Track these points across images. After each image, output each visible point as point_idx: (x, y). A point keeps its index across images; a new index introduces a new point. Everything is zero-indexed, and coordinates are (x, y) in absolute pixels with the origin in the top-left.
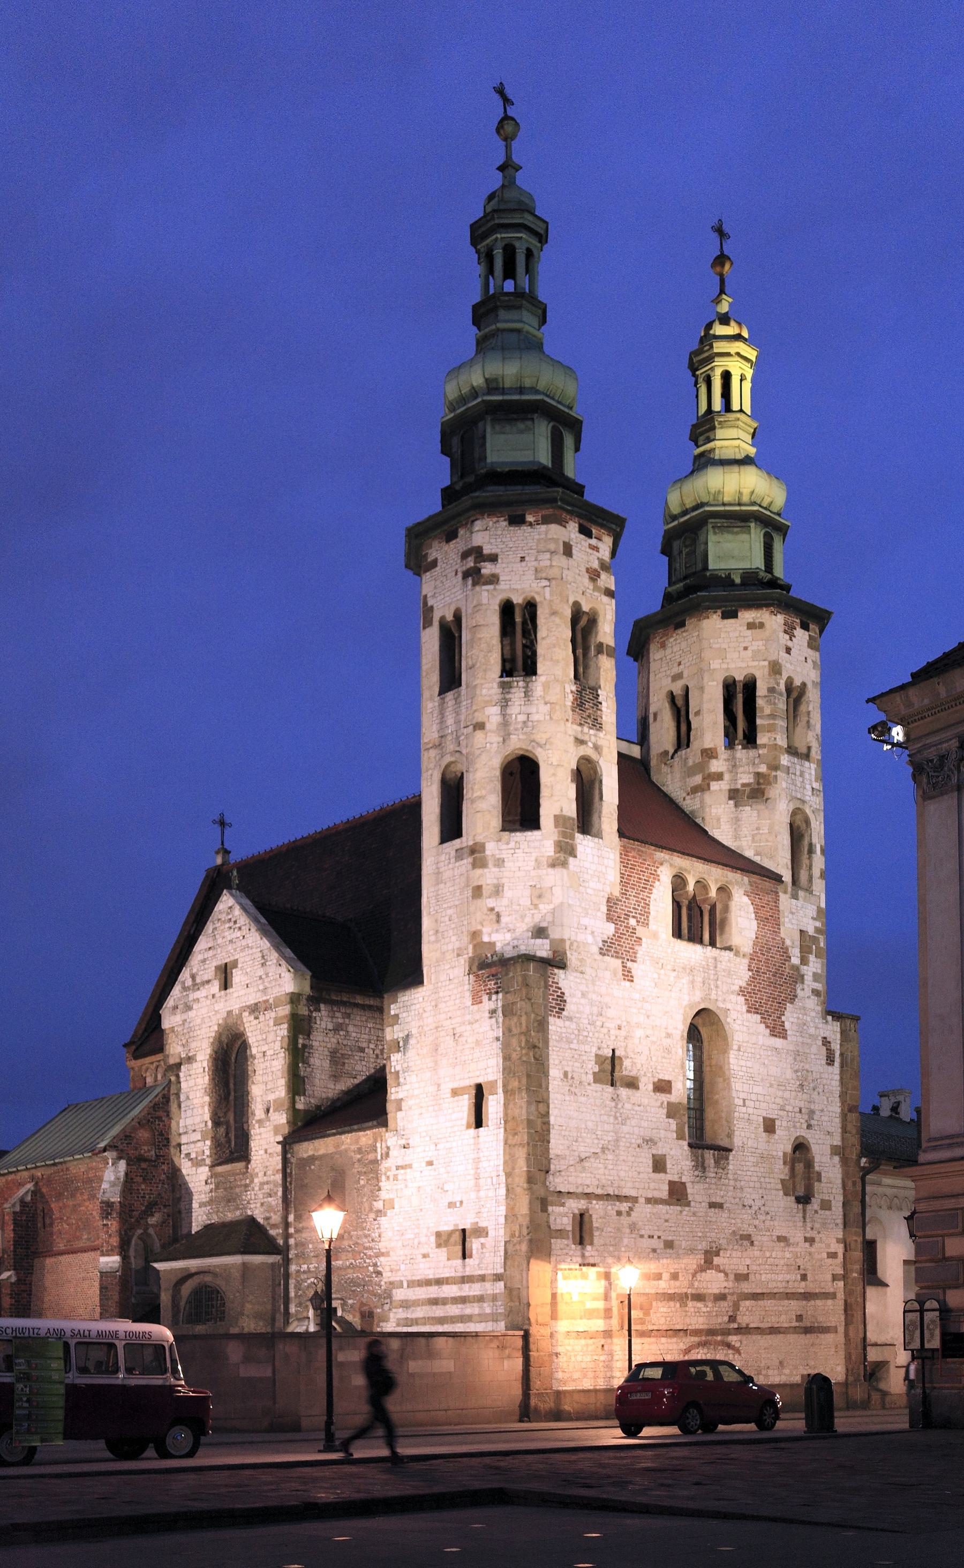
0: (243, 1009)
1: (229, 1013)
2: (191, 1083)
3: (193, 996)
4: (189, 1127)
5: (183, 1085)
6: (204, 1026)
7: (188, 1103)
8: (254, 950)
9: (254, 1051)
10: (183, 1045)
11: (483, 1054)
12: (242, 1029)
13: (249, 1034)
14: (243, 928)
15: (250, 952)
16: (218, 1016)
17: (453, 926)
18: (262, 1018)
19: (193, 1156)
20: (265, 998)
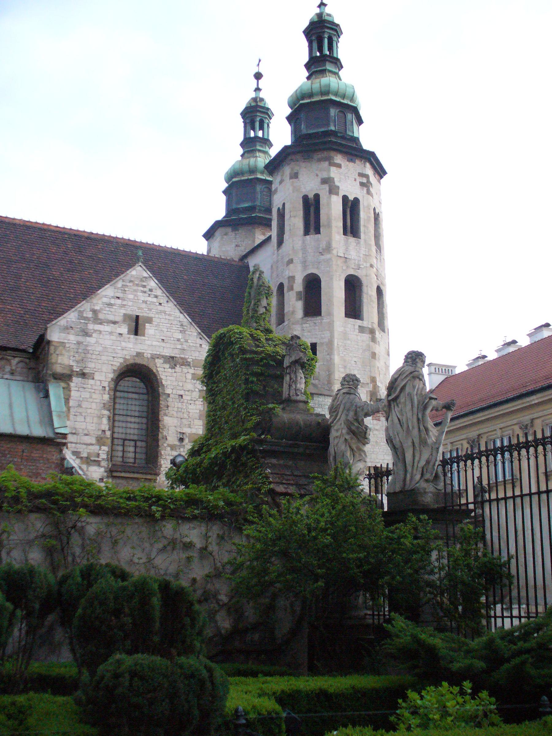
0: (154, 357)
1: (139, 354)
2: (86, 395)
3: (91, 326)
4: (81, 431)
5: (73, 393)
6: (106, 354)
7: (80, 410)
8: (172, 318)
9: (168, 391)
10: (78, 362)
11: (381, 450)
12: (155, 371)
13: (162, 377)
14: (159, 297)
15: (167, 317)
16: (125, 352)
17: (358, 369)
18: (178, 368)
19: (85, 455)
20: (182, 356)
